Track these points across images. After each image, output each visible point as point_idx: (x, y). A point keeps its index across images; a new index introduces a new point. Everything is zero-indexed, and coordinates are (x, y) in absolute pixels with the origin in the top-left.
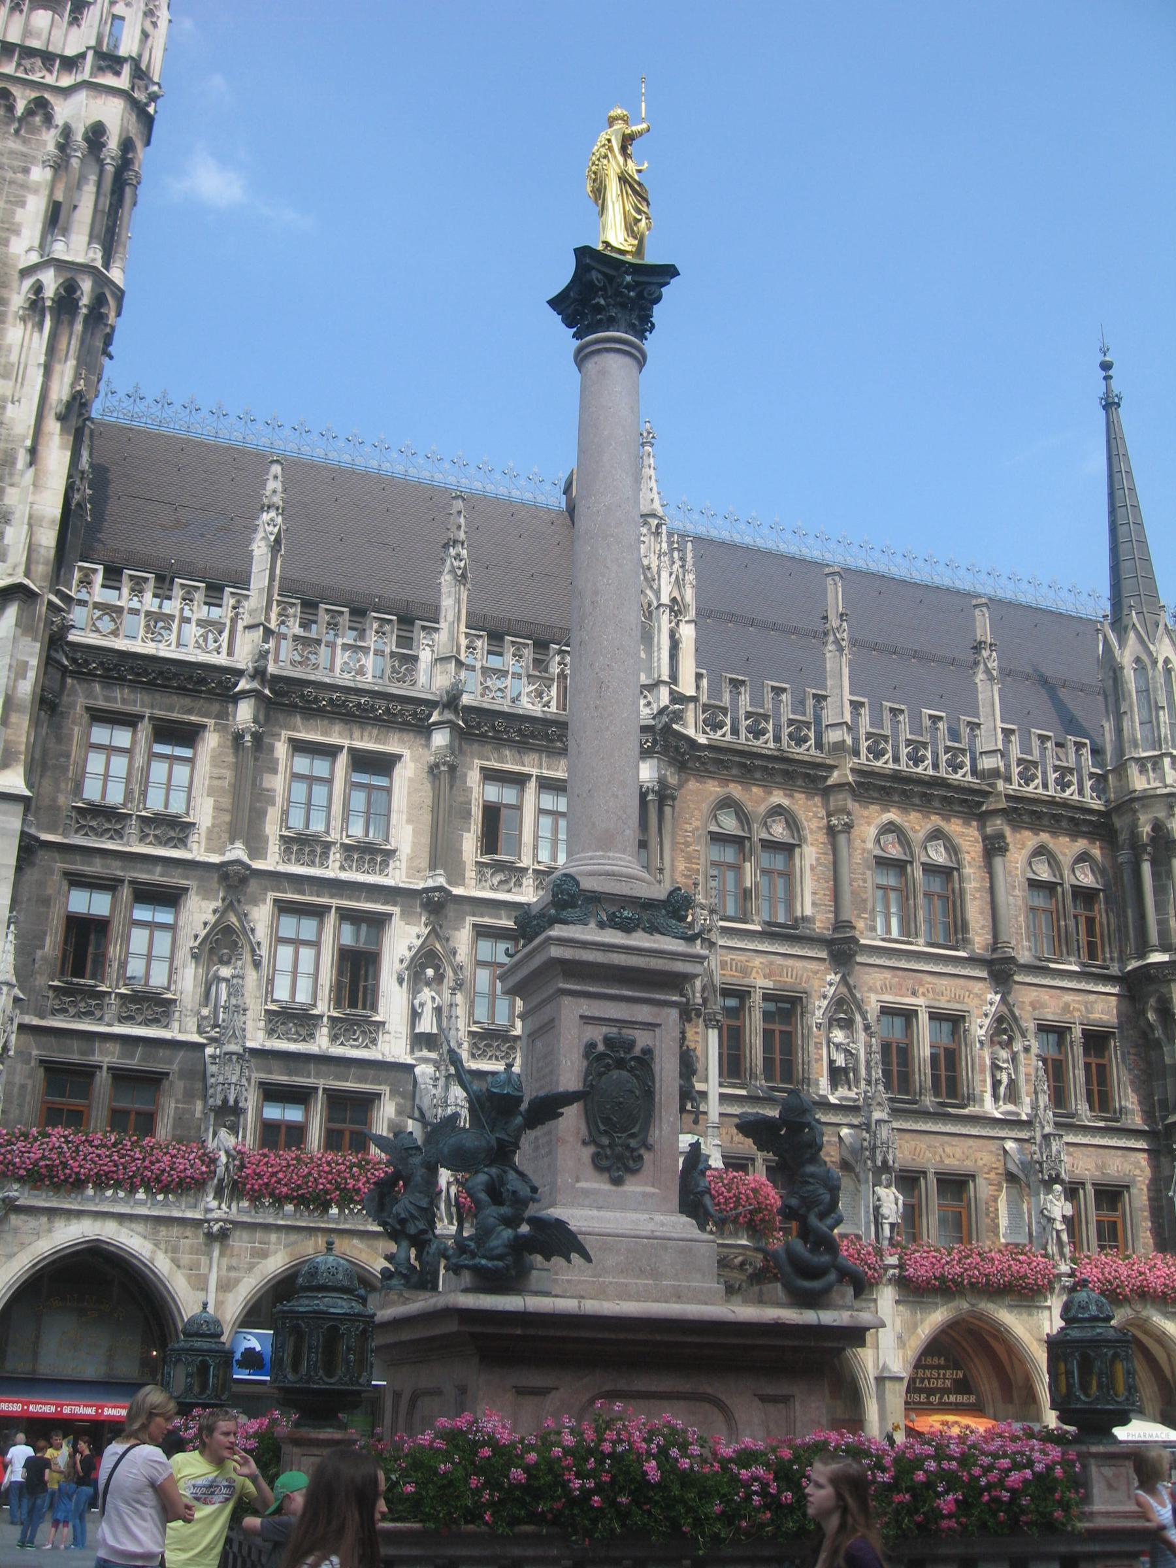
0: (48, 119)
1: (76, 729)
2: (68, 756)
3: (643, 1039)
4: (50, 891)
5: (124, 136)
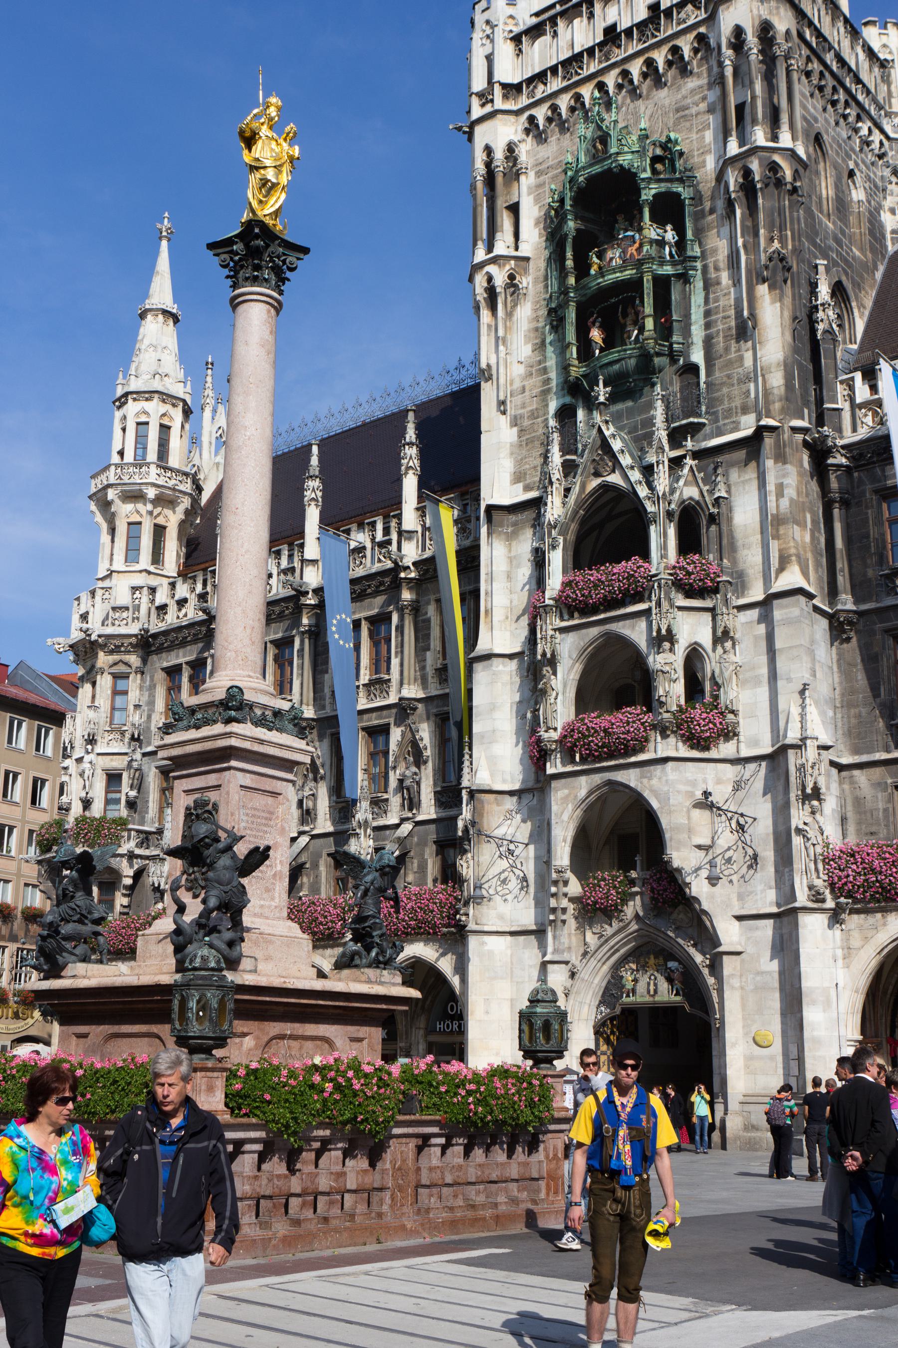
0: (708, 45)
1: (870, 511)
2: (868, 536)
3: (213, 796)
4: (876, 649)
5: (757, 23)
